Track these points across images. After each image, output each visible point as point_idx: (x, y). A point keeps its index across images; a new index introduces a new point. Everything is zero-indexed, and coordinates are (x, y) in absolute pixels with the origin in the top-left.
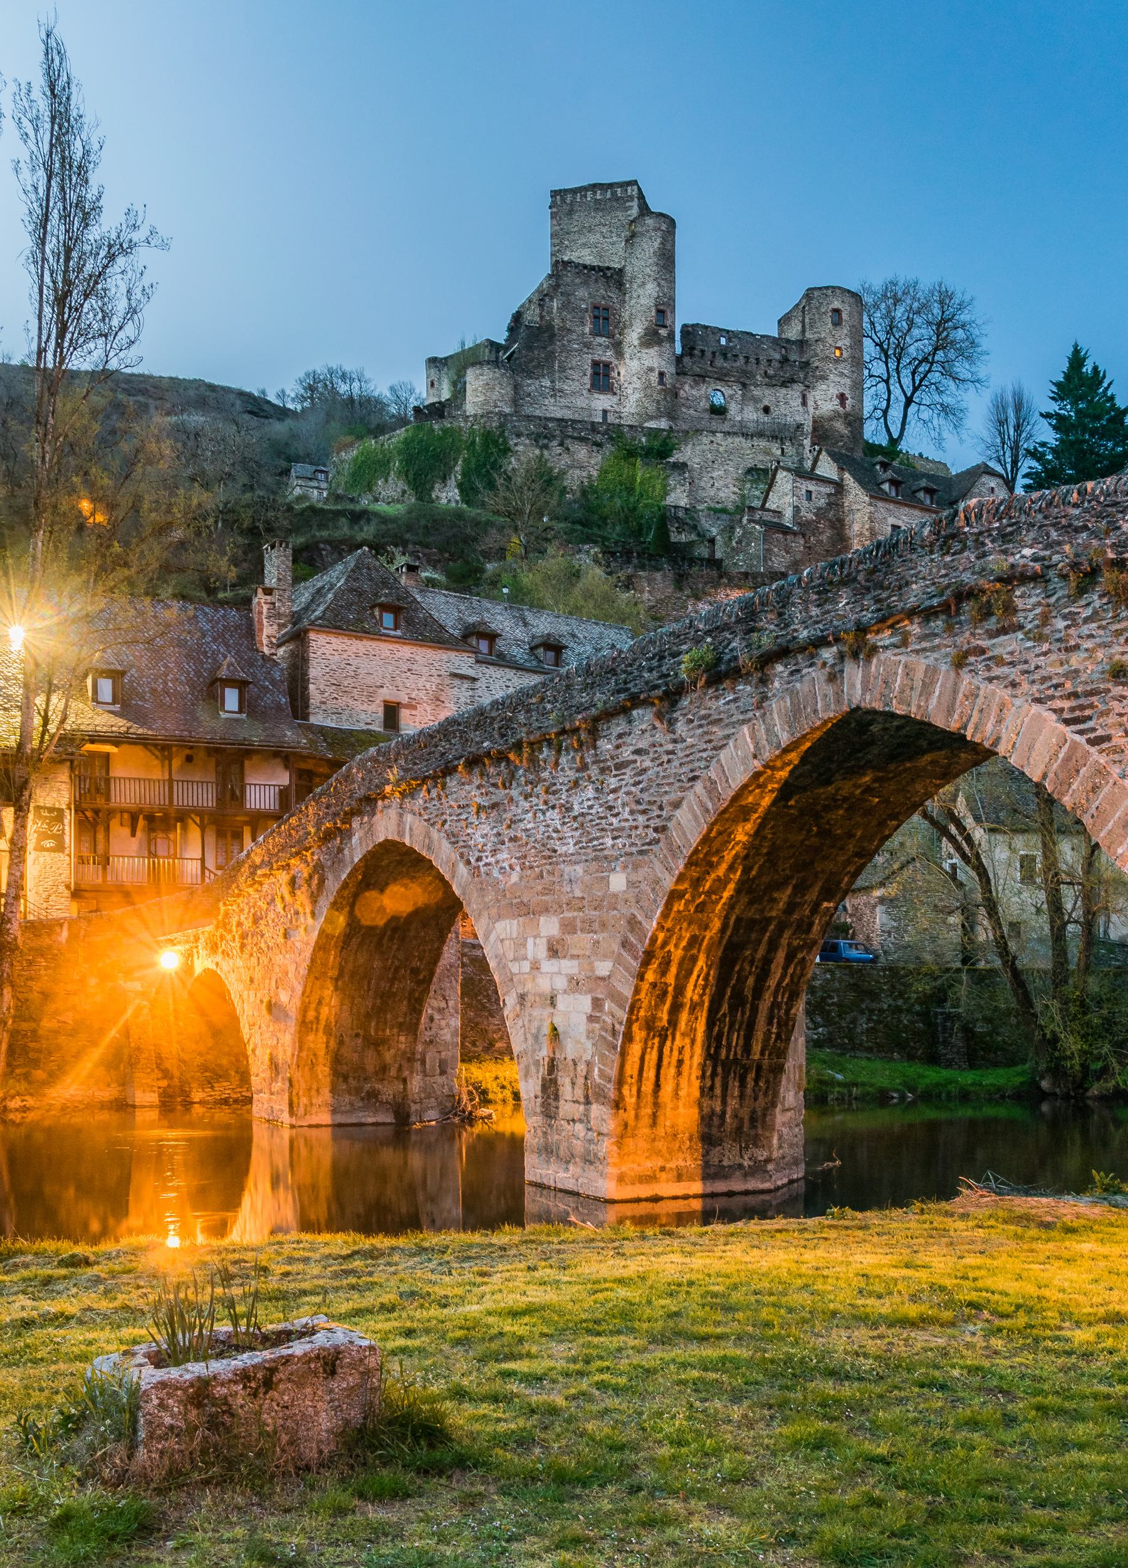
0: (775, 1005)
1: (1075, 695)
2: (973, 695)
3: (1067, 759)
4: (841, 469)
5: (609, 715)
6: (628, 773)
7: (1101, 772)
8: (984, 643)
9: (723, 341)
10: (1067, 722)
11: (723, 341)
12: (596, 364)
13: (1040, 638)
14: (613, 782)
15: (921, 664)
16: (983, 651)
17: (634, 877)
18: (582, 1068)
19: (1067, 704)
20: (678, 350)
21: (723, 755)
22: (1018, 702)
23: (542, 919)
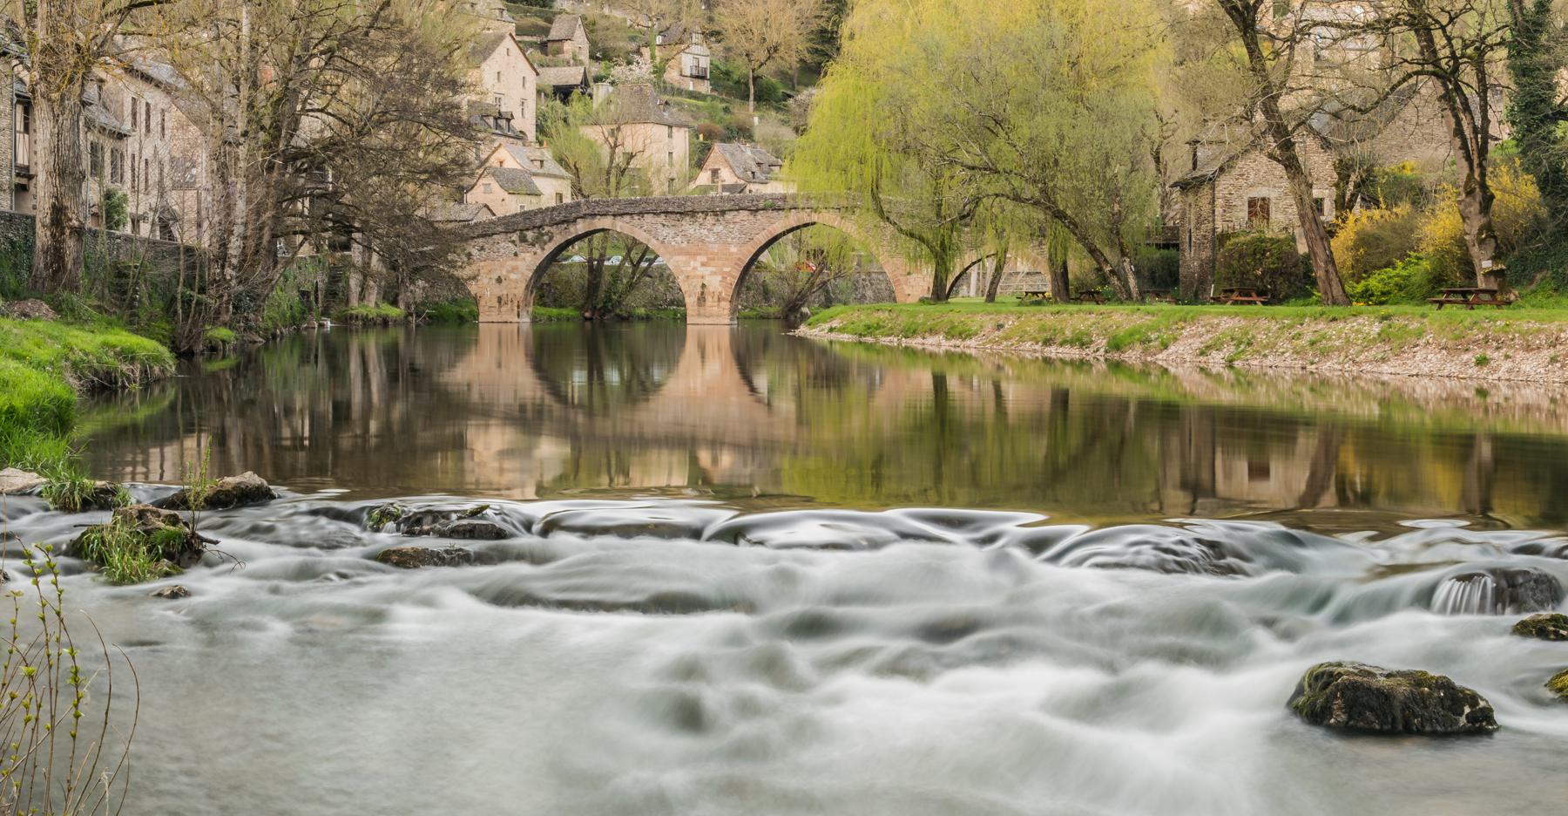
5: (730, 210)
6: (738, 225)
18: (717, 294)
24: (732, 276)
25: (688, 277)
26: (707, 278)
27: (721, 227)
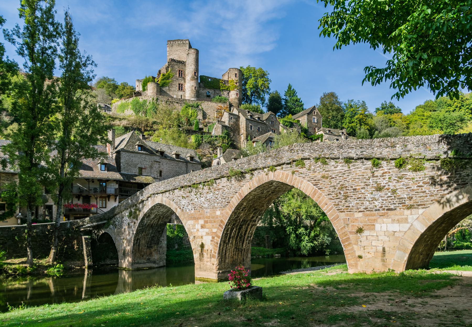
0: (248, 237)
1: (316, 180)
2: (296, 179)
3: (314, 191)
4: (239, 112)
6: (221, 191)
7: (321, 194)
8: (298, 170)
9: (210, 80)
10: (314, 185)
11: (210, 80)
12: (179, 84)
13: (309, 169)
14: (217, 193)
15: (286, 172)
16: (298, 171)
17: (222, 212)
18: (209, 251)
19: (314, 182)
20: (199, 81)
21: (243, 188)
22: (305, 181)
23: (200, 220)
24: (218, 237)
25: (194, 237)
26: (204, 237)
27: (212, 194)
